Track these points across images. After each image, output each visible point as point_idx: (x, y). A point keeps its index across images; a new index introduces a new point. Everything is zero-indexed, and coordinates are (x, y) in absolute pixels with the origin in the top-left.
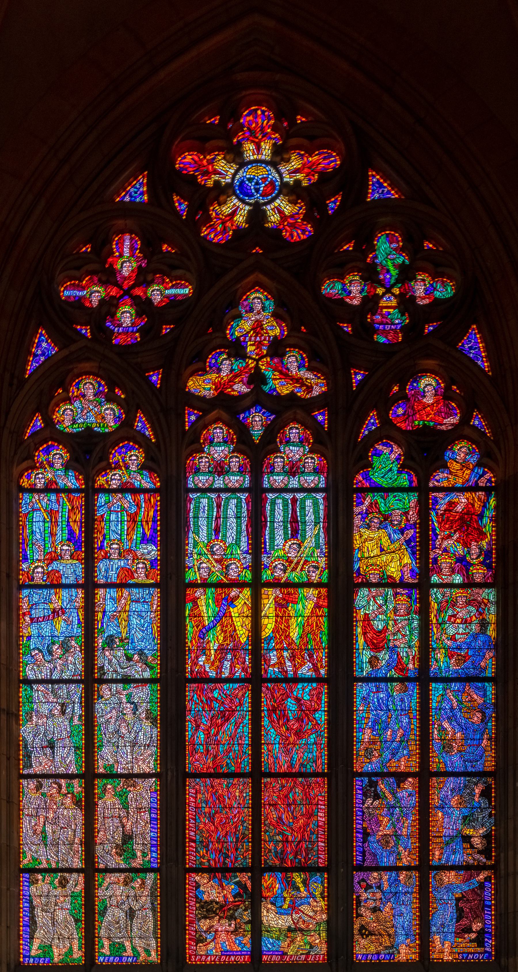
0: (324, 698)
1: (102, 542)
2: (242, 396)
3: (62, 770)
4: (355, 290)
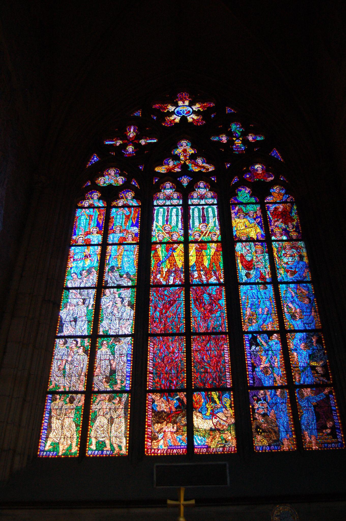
0: (224, 293)
1: (112, 227)
3: (79, 334)
4: (224, 139)
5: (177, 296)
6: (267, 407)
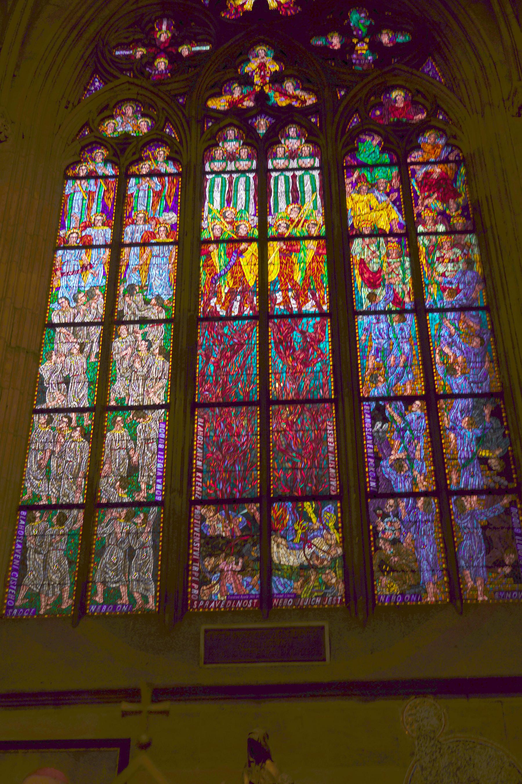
0: (328, 331)
1: (131, 213)
2: (249, 109)
4: (336, 42)
5: (246, 335)
6: (400, 529)
